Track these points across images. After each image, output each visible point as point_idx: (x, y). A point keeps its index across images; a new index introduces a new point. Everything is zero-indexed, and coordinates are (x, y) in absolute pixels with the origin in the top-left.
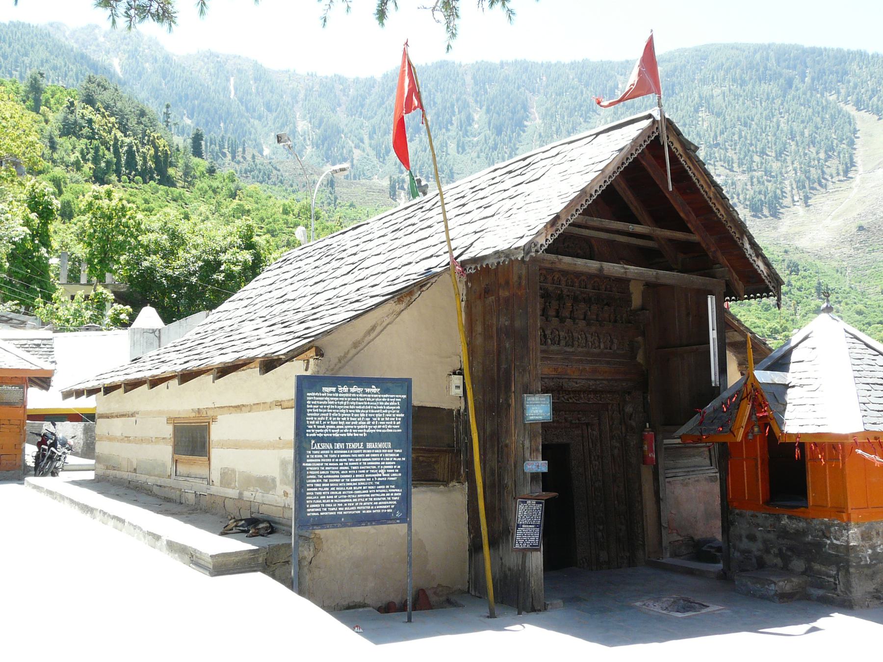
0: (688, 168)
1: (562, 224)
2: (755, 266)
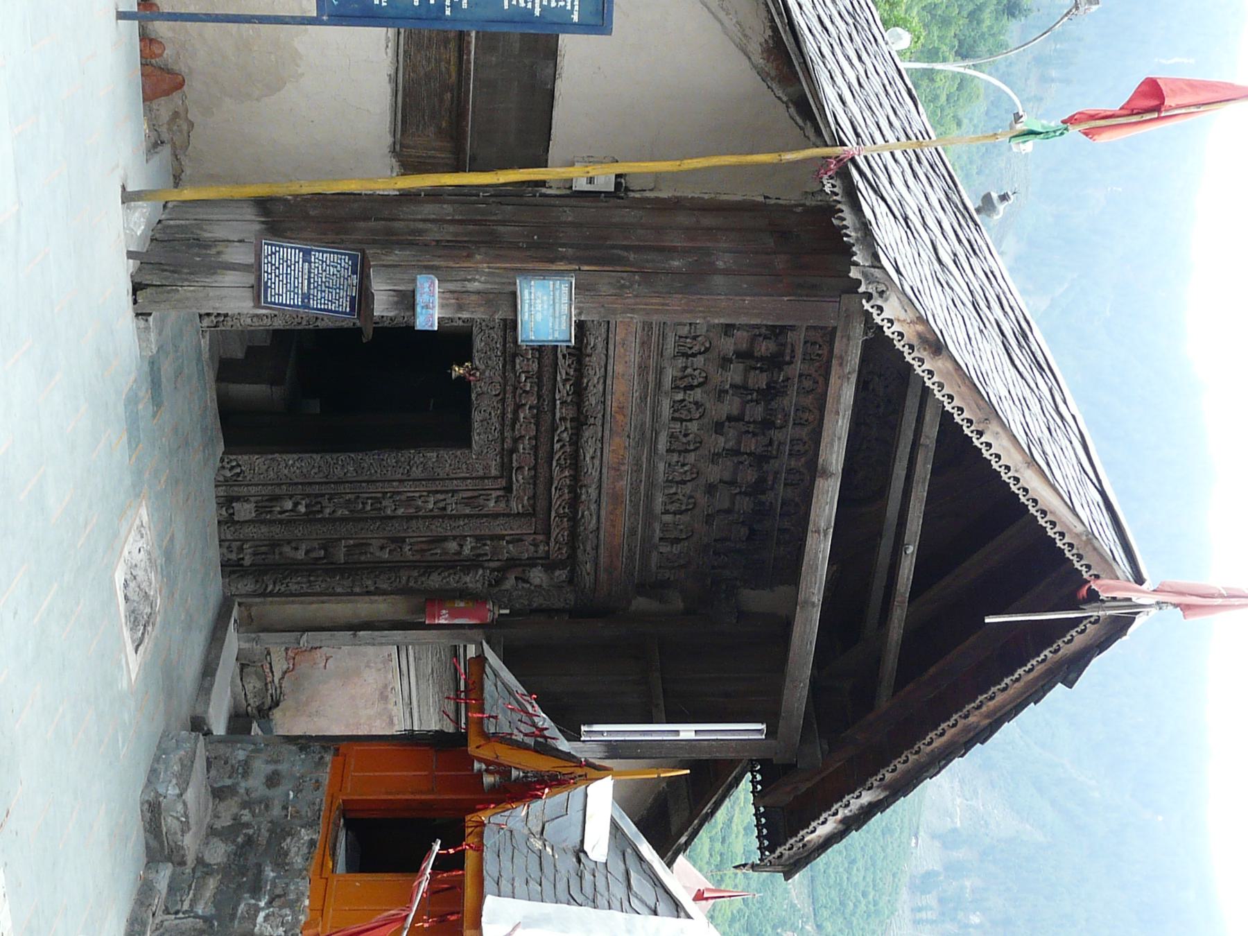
0: (1029, 666)
1: (921, 360)
2: (824, 815)
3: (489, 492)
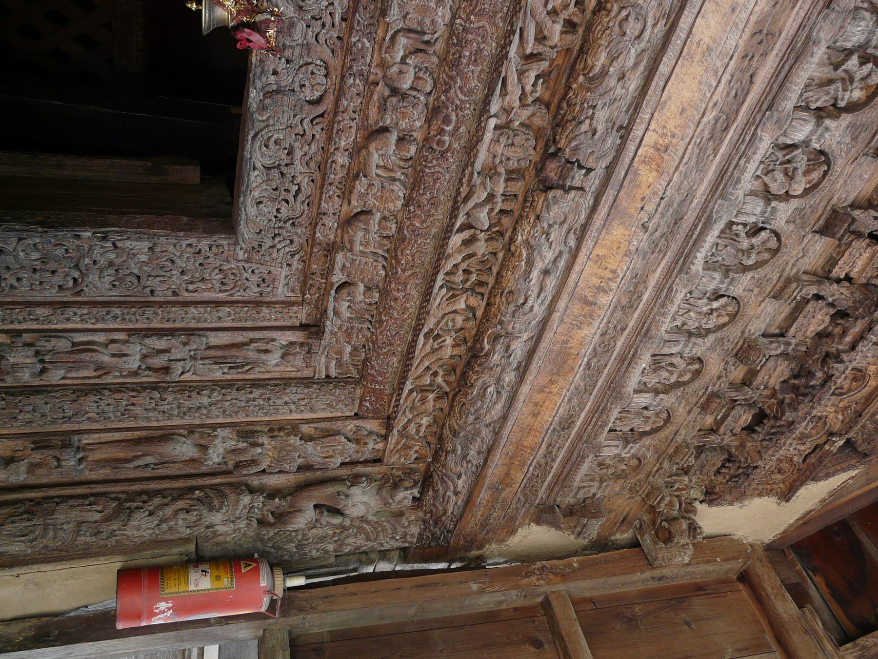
3: (268, 334)
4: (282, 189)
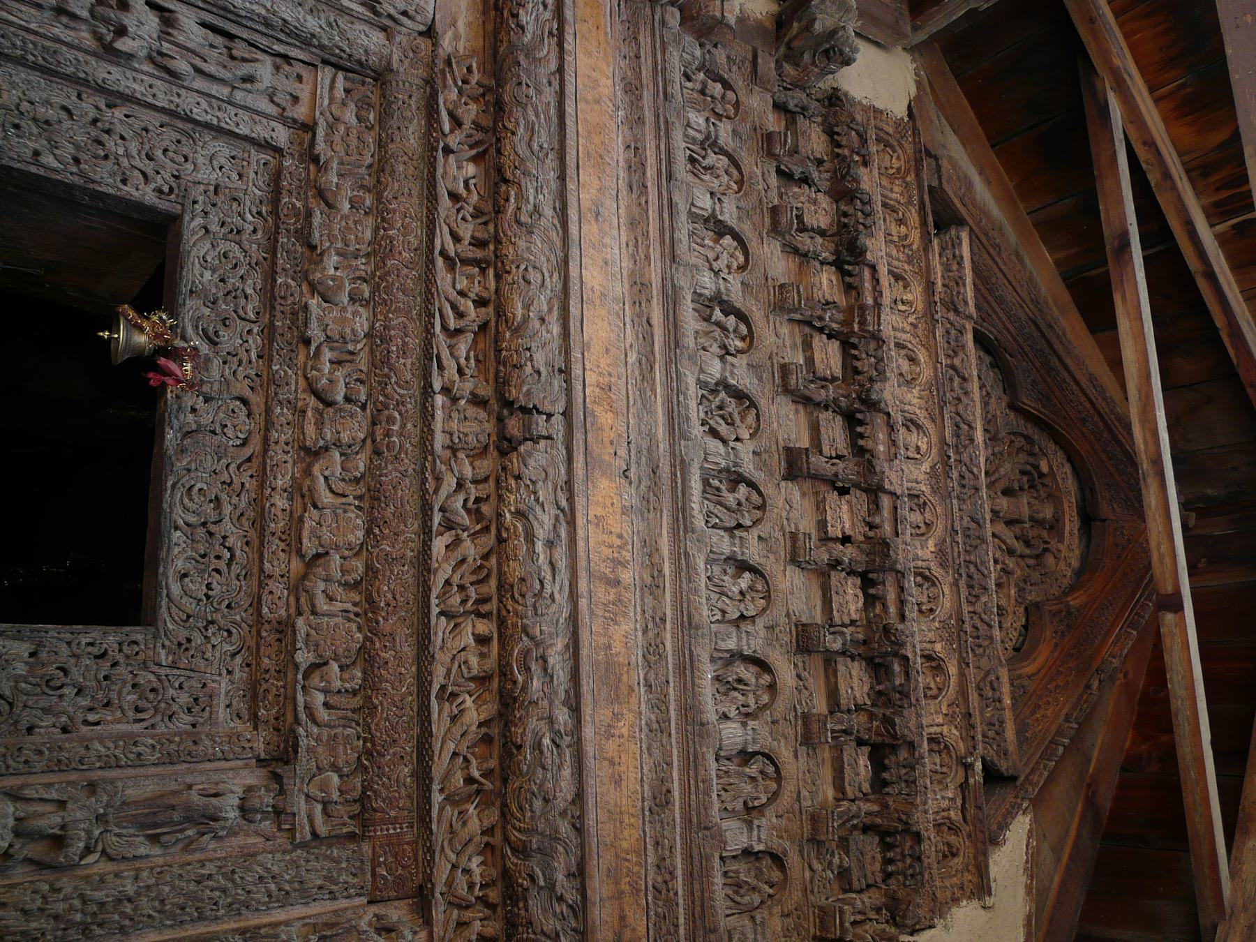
3: (216, 777)
4: (212, 556)
